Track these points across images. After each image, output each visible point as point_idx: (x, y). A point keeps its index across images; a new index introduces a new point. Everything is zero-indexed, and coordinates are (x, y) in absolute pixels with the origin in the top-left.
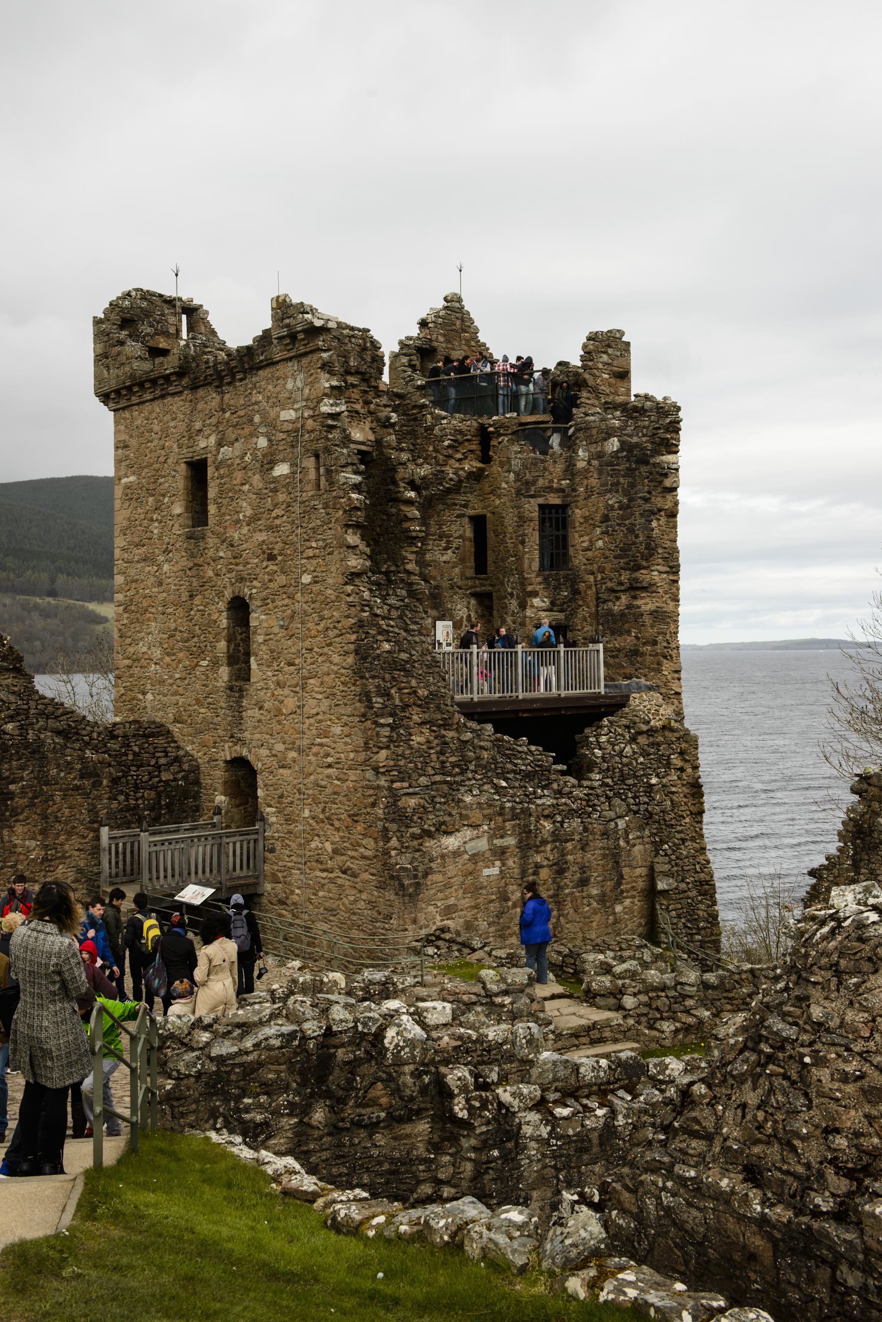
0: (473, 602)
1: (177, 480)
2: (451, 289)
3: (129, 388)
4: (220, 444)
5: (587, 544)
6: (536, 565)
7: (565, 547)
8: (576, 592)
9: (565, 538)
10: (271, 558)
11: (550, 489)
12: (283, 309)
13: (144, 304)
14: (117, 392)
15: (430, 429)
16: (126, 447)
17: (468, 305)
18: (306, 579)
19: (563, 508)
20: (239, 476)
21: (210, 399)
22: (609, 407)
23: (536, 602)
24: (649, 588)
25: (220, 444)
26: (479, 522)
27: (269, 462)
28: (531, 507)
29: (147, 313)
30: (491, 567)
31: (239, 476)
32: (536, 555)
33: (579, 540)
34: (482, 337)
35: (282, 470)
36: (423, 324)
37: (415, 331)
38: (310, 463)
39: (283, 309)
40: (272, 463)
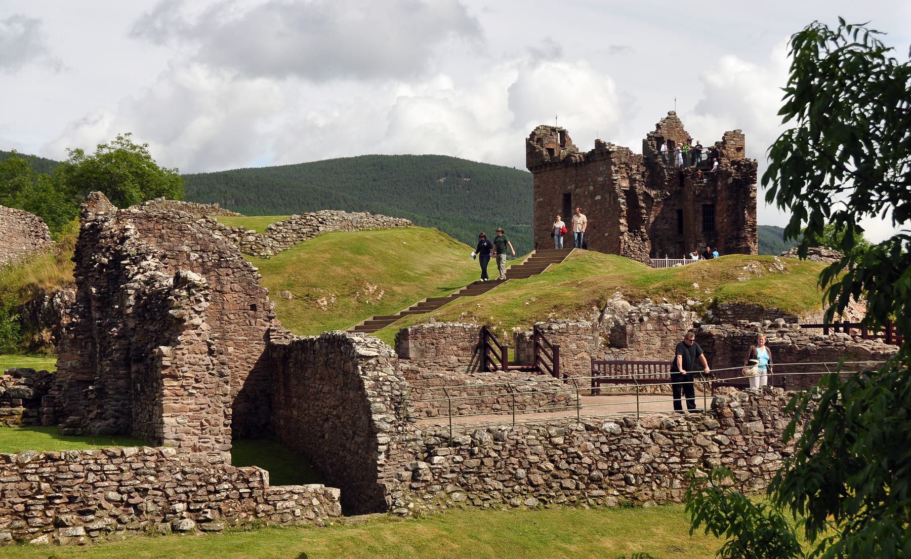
0: (678, 246)
1: (560, 200)
2: (671, 109)
3: (541, 167)
4: (576, 188)
5: (722, 220)
6: (701, 230)
7: (713, 221)
8: (717, 240)
9: (713, 218)
10: (595, 228)
11: (707, 198)
12: (598, 143)
13: (544, 132)
14: (536, 167)
15: (659, 173)
16: (539, 187)
17: (678, 116)
18: (606, 234)
19: (713, 206)
20: (583, 199)
21: (573, 171)
22: (733, 163)
23: (701, 244)
24: (745, 238)
25: (576, 188)
26: (680, 212)
27: (593, 195)
28: (699, 206)
29: (546, 135)
30: (684, 231)
31: (583, 199)
32: (701, 225)
33: (718, 219)
34: (685, 129)
35: (598, 198)
36: (658, 126)
37: (654, 129)
38: (607, 196)
39: (598, 143)
40: (595, 195)
